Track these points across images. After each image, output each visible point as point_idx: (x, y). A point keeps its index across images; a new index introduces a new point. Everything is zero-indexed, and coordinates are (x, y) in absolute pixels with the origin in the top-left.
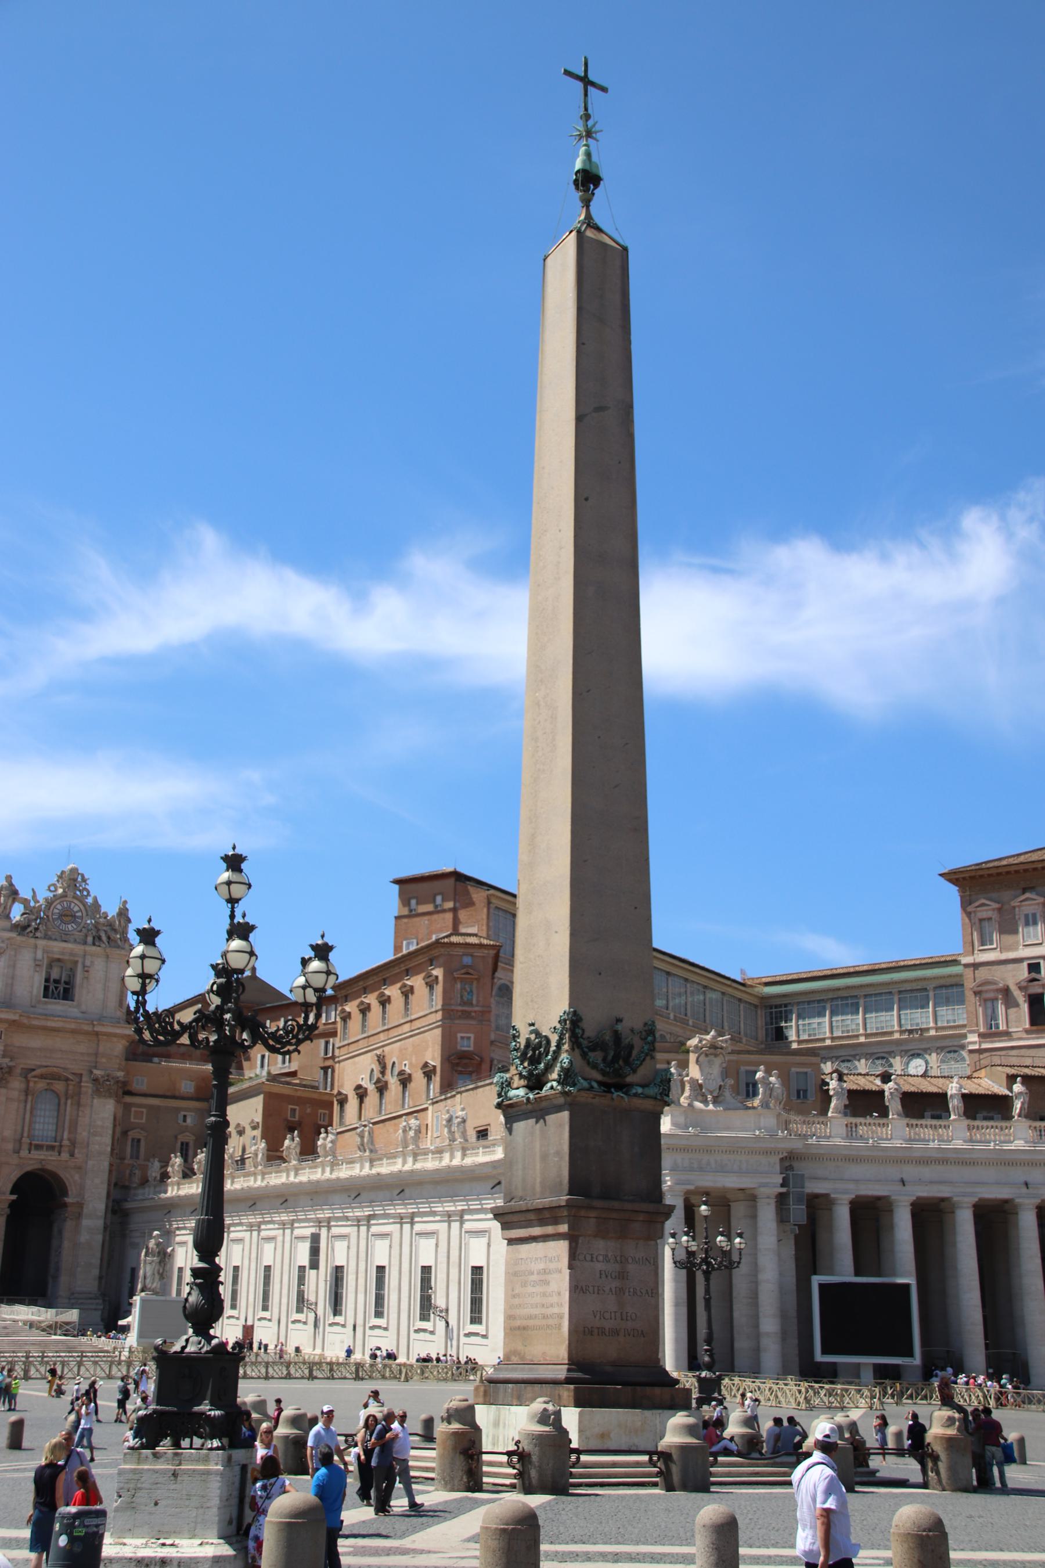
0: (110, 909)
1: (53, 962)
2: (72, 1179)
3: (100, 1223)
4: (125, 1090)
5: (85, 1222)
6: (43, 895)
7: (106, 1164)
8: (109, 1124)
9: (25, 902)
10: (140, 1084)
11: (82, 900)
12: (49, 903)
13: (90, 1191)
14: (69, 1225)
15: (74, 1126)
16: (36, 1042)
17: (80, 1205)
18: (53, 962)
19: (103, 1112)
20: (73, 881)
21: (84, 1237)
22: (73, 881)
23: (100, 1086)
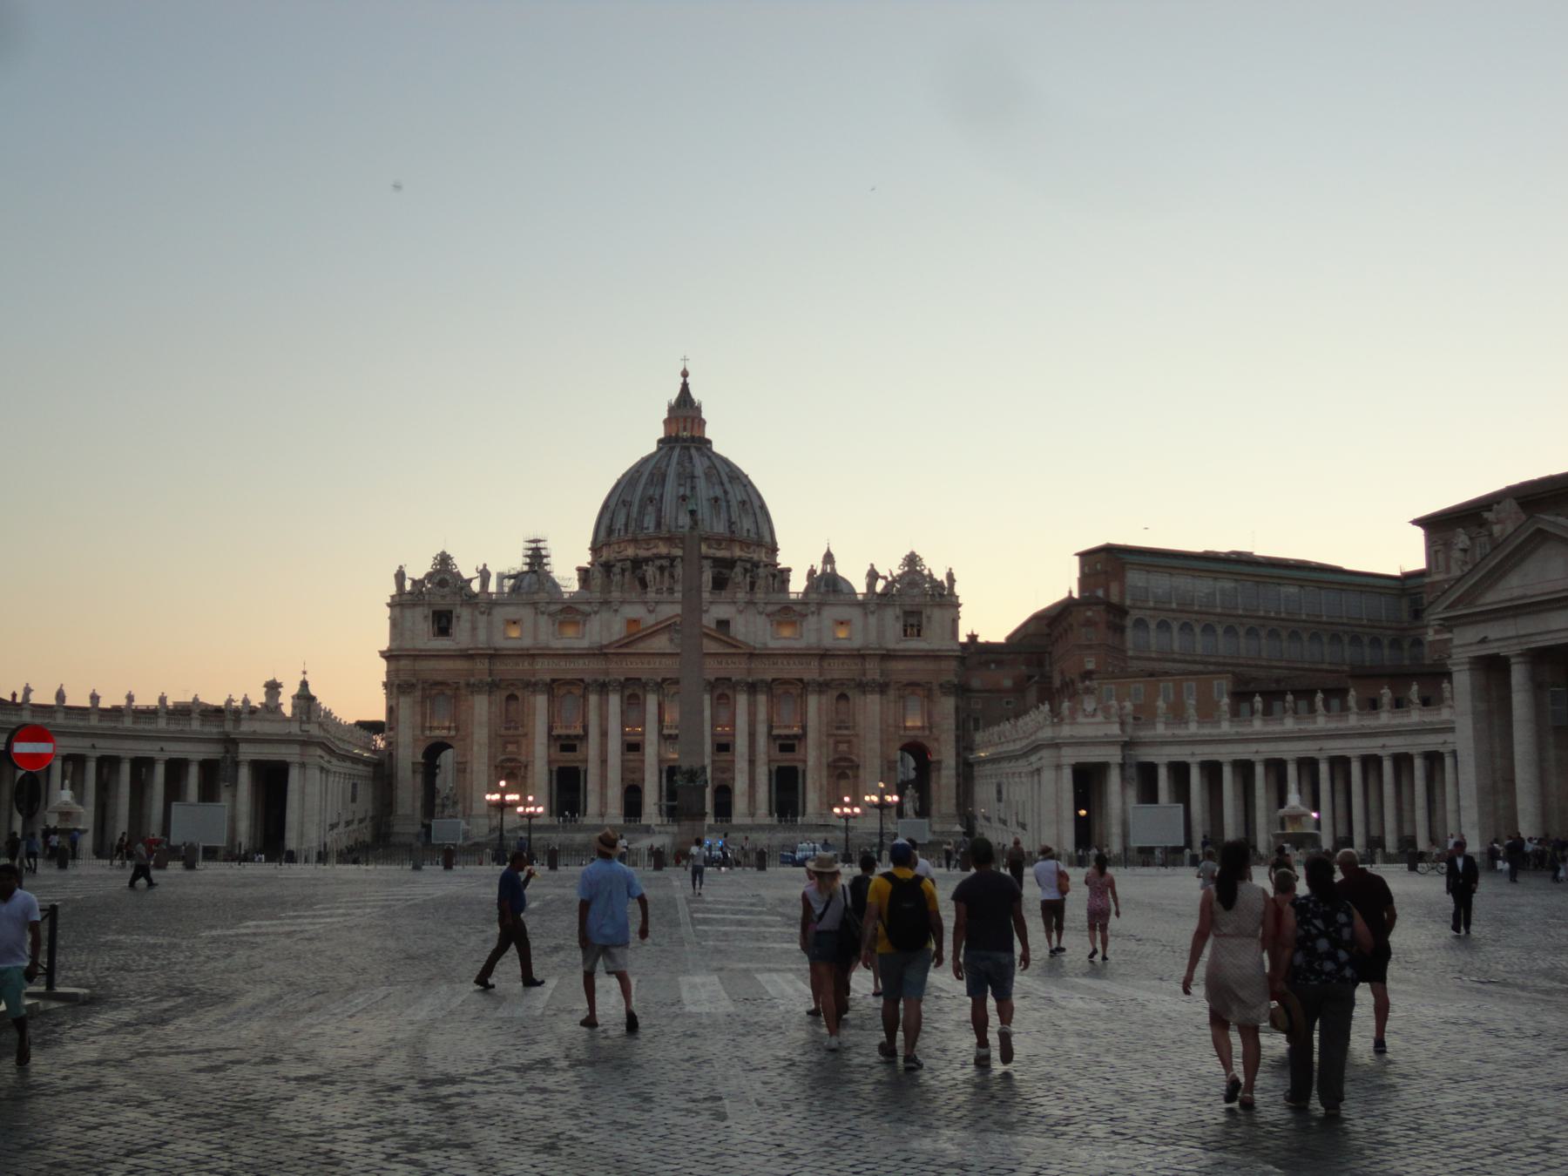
0: (940, 576)
1: (907, 614)
2: (931, 745)
3: (953, 772)
4: (961, 690)
5: (944, 773)
6: (897, 572)
7: (953, 738)
8: (952, 711)
9: (885, 578)
10: (976, 683)
11: (920, 573)
12: (901, 576)
13: (946, 754)
14: (934, 775)
15: (930, 715)
16: (900, 666)
17: (939, 762)
18: (907, 614)
19: (948, 705)
20: (912, 560)
21: (944, 781)
22: (912, 560)
23: (947, 689)
